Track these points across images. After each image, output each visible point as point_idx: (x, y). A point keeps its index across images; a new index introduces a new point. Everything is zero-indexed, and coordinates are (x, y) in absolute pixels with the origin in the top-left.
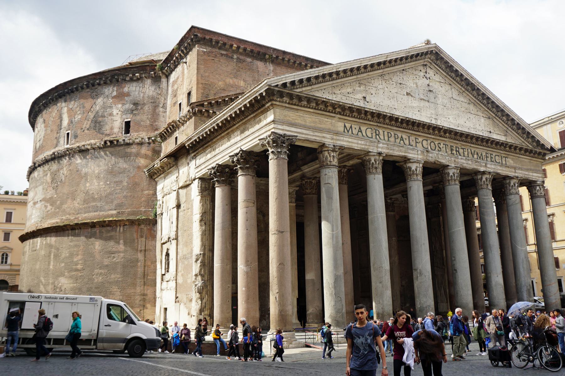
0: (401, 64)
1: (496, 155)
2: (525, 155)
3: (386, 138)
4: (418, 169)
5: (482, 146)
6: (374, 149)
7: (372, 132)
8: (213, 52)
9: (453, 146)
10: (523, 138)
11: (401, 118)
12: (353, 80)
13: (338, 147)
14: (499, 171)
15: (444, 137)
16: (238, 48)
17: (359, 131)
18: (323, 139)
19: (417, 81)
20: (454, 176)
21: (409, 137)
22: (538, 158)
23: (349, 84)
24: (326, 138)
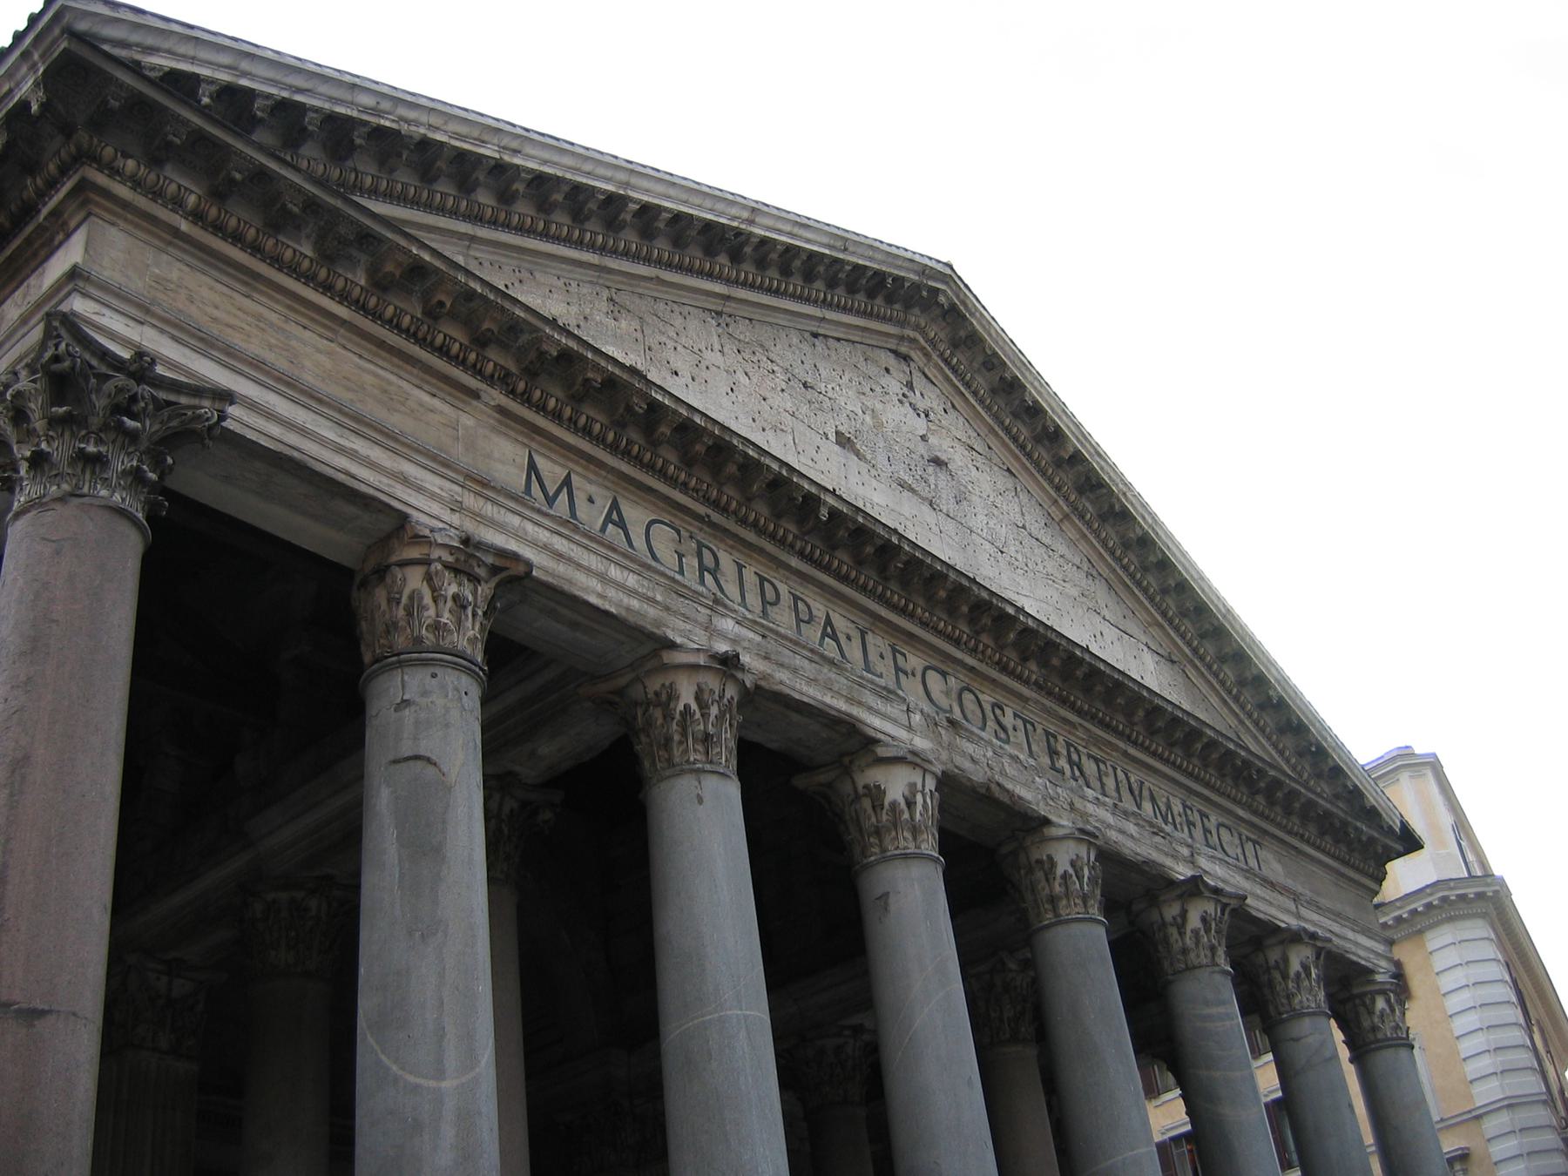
3: (754, 600)
4: (919, 798)
7: (682, 549)
11: (830, 500)
13: (489, 560)
15: (1019, 678)
17: (608, 519)
18: (400, 491)
19: (879, 406)
20: (1080, 878)
21: (863, 634)
23: (560, 283)
24: (420, 489)
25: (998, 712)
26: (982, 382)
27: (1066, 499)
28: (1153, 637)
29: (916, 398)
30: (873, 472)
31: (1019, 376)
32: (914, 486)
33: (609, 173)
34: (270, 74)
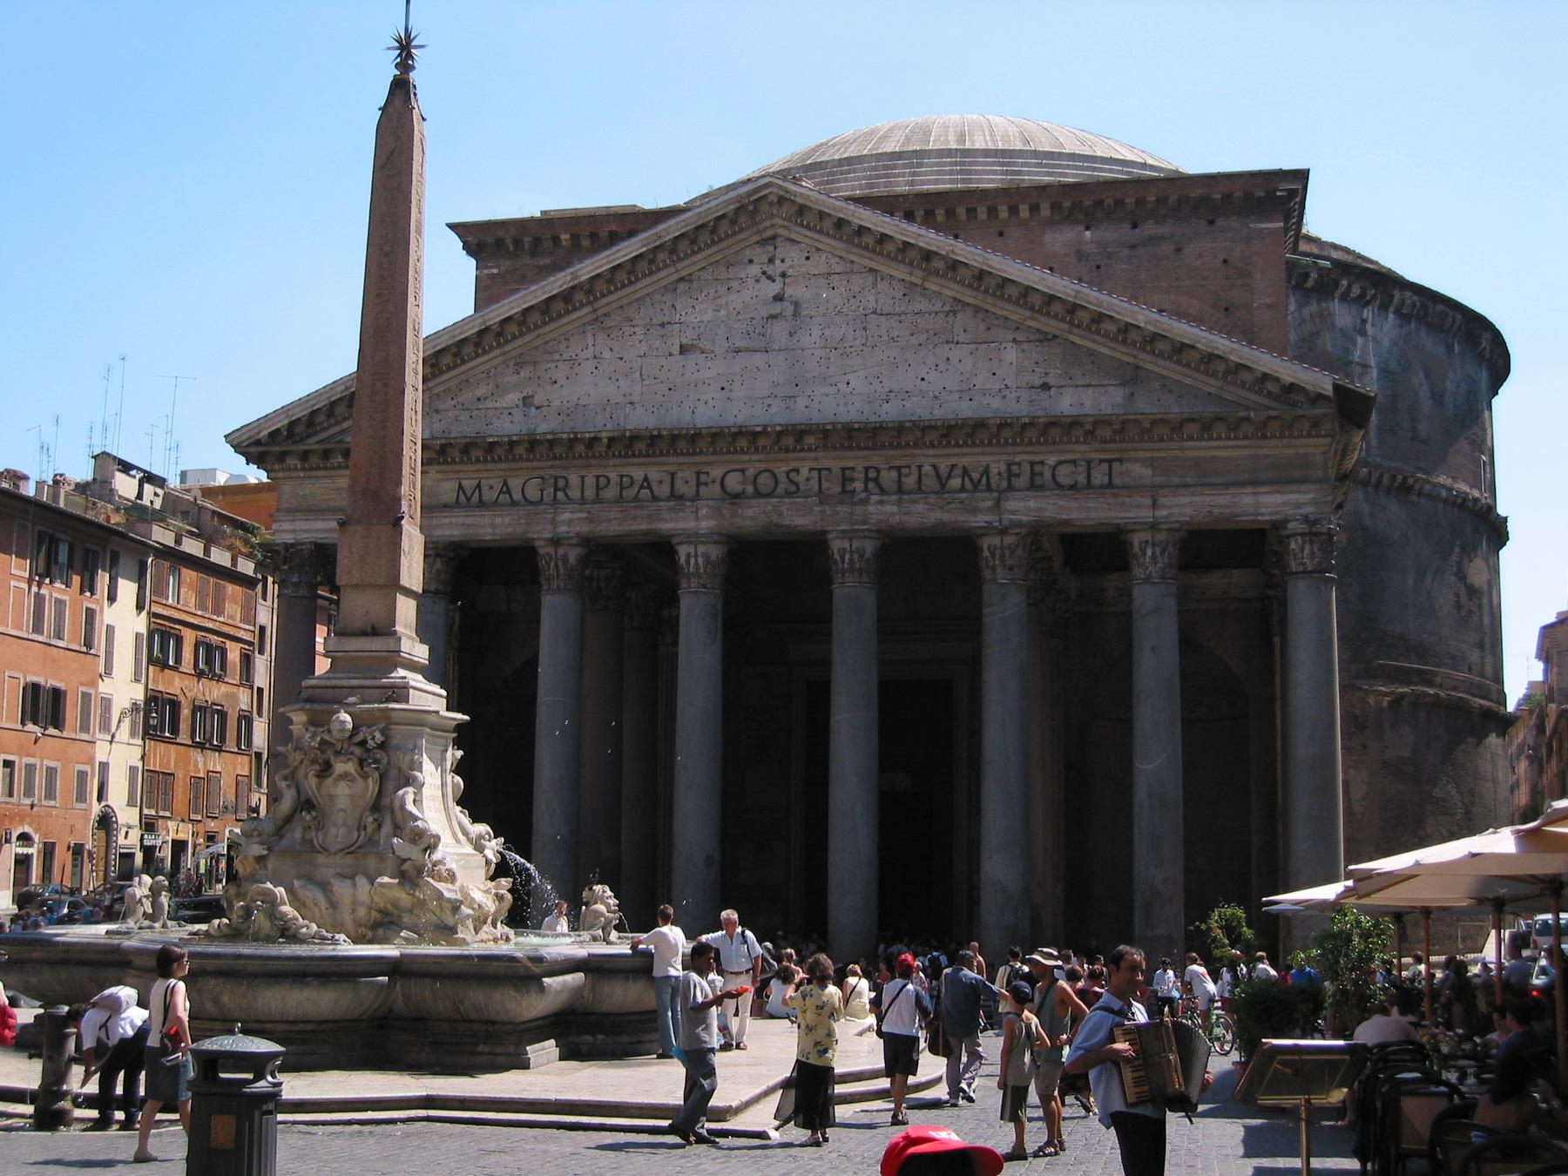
0: (659, 269)
1: (1061, 463)
2: (1210, 439)
3: (590, 493)
4: (692, 560)
5: (974, 445)
6: (539, 531)
8: (516, 270)
9: (853, 469)
10: (1214, 375)
11: (604, 435)
12: (495, 362)
14: (1064, 517)
15: (802, 450)
16: (575, 238)
17: (501, 492)
22: (1292, 437)
23: (483, 376)
25: (792, 475)
26: (828, 224)
27: (920, 268)
28: (1030, 327)
29: (778, 267)
30: (712, 356)
31: (842, 216)
32: (750, 345)
33: (471, 325)
34: (302, 408)
